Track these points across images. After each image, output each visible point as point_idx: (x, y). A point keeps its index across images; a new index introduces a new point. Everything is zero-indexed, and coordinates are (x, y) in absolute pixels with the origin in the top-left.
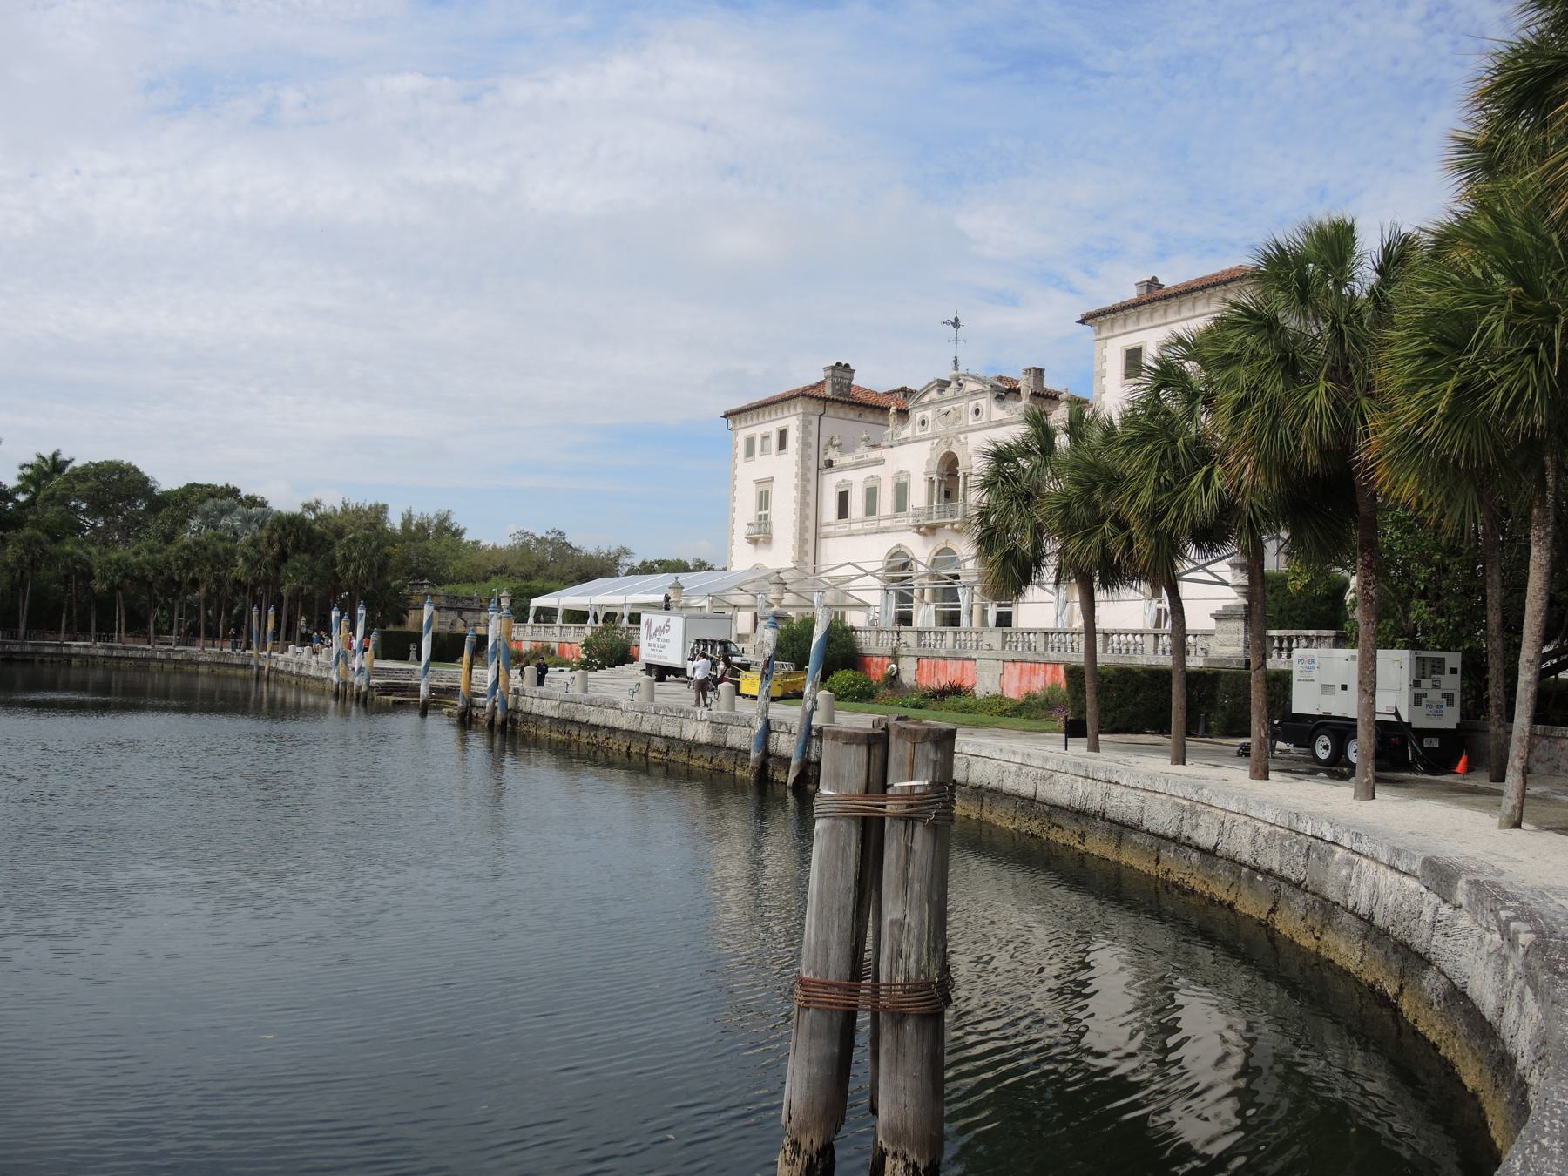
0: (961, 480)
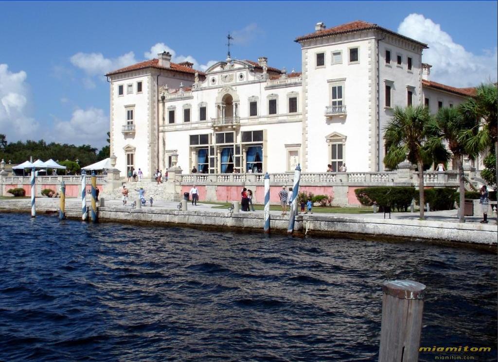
0: (234, 106)
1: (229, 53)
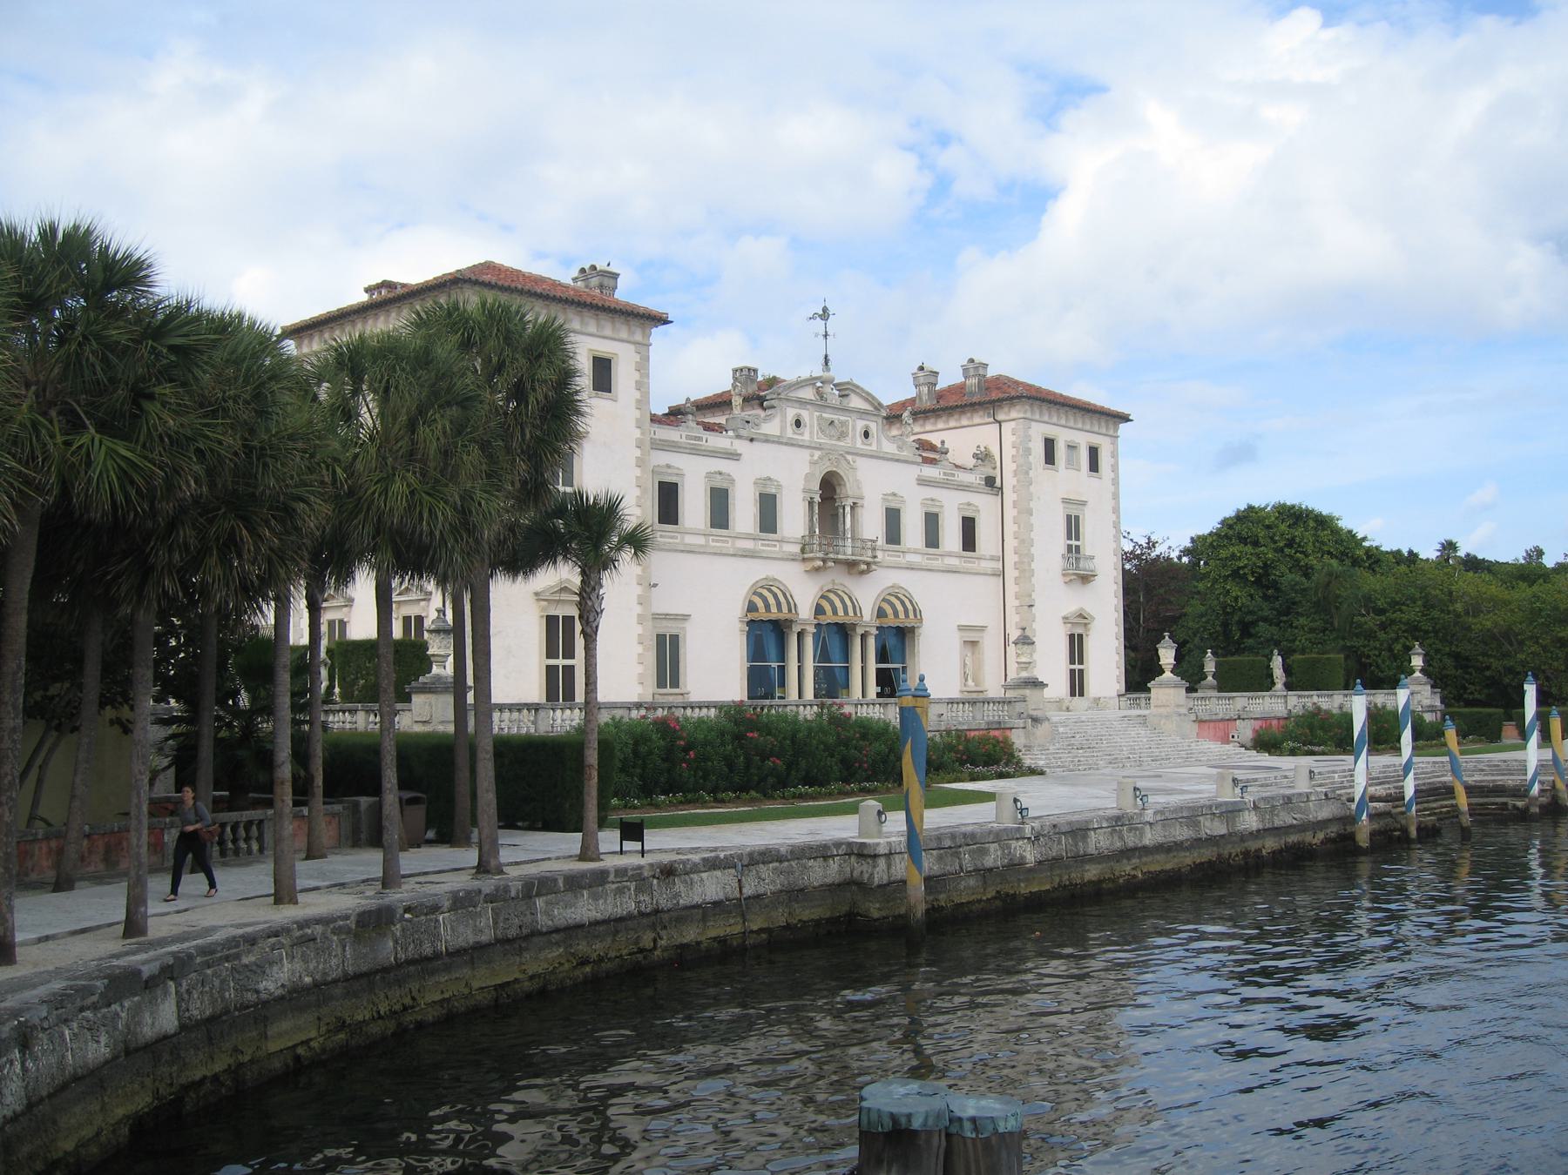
1: (826, 356)
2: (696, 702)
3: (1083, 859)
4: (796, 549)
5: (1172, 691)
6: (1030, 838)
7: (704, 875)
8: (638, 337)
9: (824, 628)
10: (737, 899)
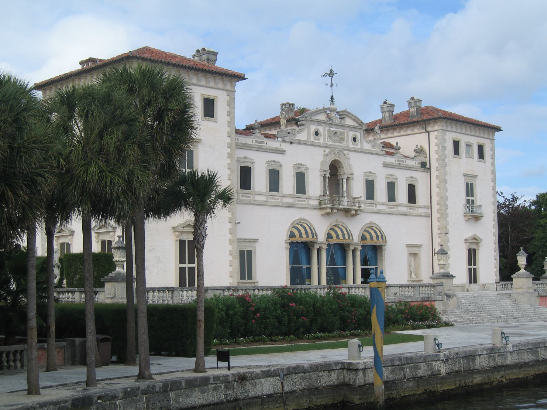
1: (332, 97)
2: (261, 287)
3: (473, 372)
4: (316, 203)
5: (525, 280)
6: (443, 360)
7: (262, 380)
8: (228, 87)
9: (332, 246)
10: (280, 393)
